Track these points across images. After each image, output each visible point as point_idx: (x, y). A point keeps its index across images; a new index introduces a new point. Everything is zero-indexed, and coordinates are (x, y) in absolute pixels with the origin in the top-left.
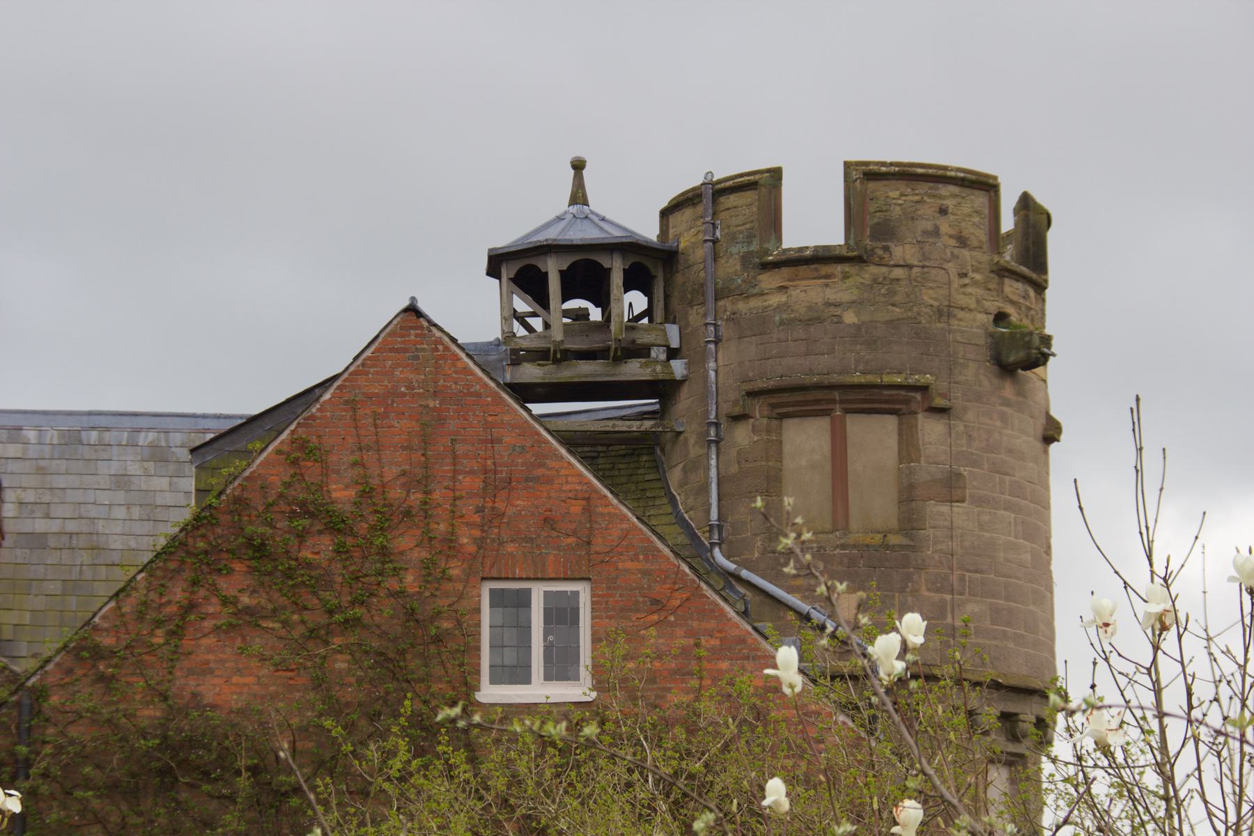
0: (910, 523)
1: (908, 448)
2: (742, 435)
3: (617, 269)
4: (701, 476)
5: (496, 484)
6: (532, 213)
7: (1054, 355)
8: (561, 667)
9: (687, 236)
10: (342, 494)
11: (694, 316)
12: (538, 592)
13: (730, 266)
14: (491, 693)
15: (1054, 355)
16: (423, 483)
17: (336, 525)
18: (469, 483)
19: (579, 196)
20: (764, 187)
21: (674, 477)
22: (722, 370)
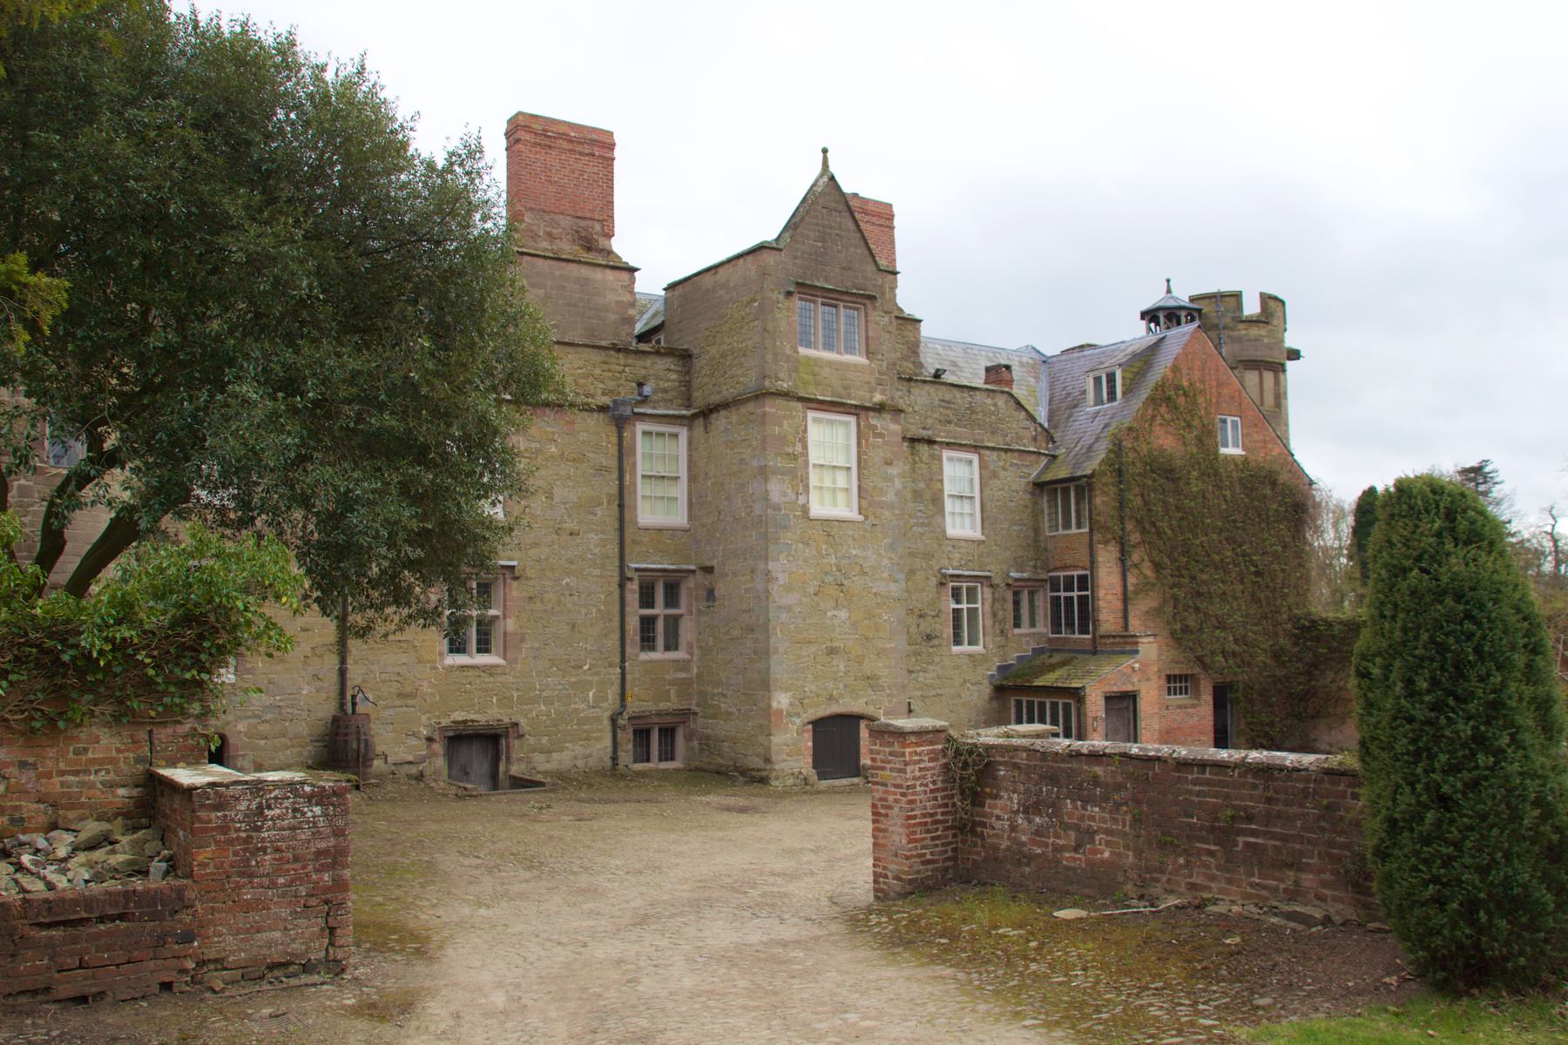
3: (1183, 314)
5: (1219, 385)
6: (1154, 297)
7: (1294, 355)
9: (1206, 307)
10: (1185, 384)
12: (1229, 419)
13: (1227, 320)
14: (1223, 451)
15: (1294, 355)
16: (1203, 382)
18: (1214, 383)
19: (1169, 291)
20: (1237, 296)
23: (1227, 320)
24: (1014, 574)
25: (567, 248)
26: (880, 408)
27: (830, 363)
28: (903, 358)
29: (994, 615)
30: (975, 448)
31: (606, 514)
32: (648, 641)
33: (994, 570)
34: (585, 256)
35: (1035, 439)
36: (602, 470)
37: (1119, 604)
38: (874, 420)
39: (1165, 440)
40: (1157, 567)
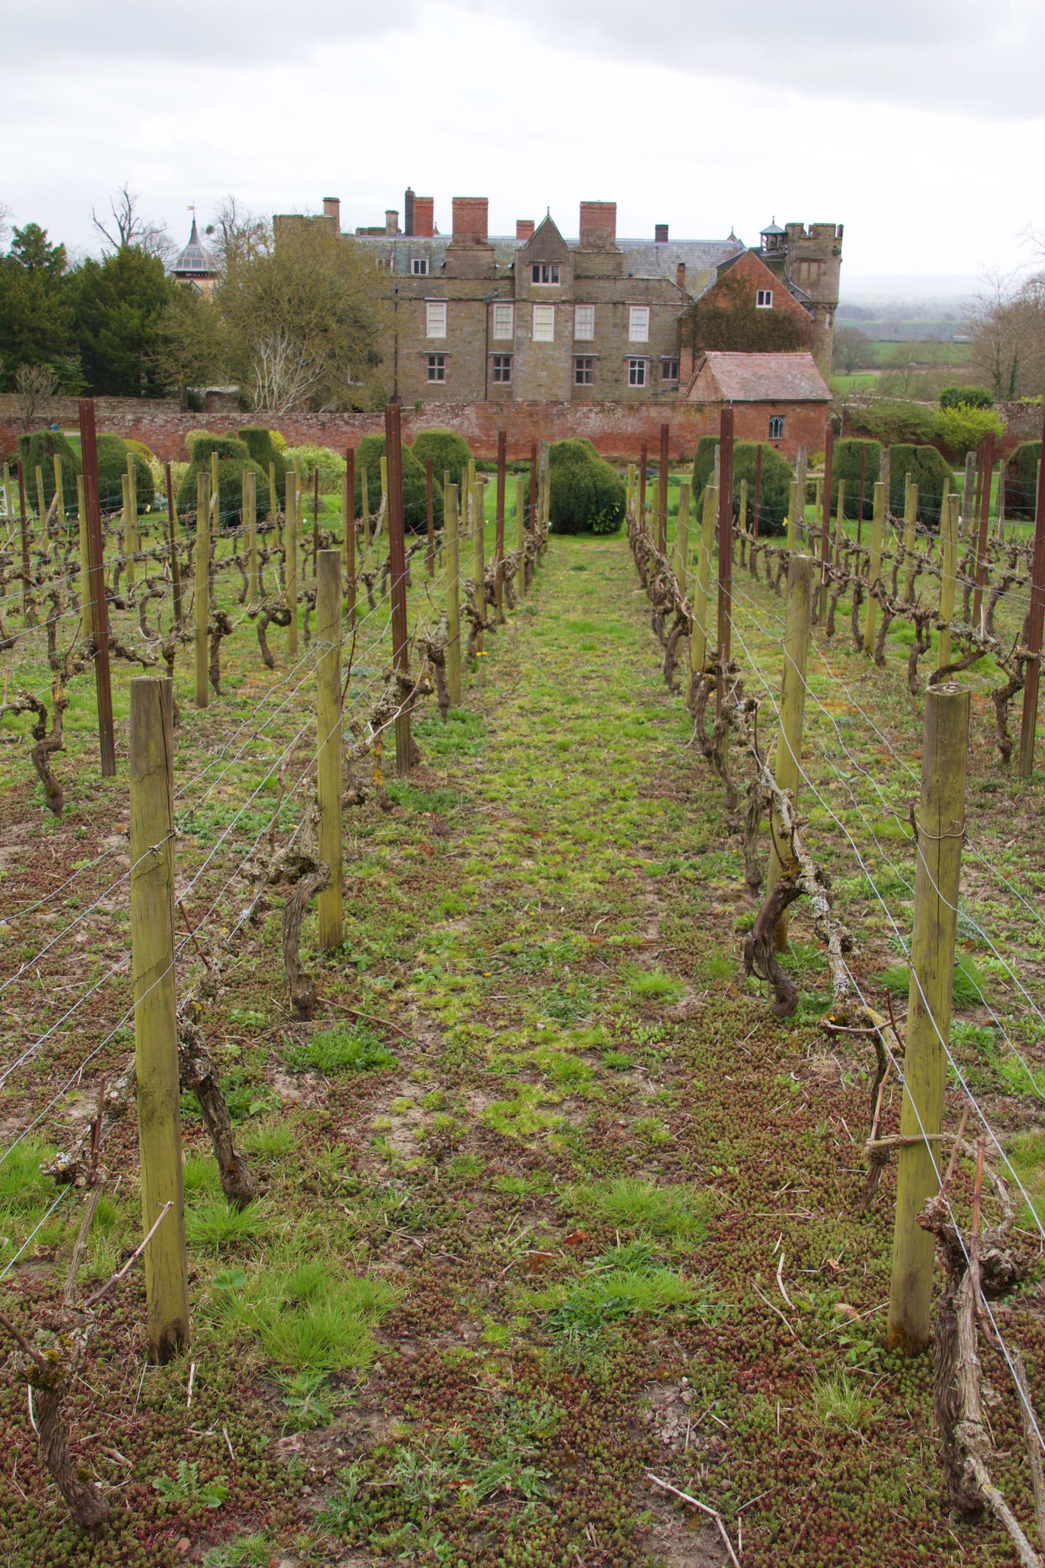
0: (819, 279)
4: (789, 270)
8: (768, 302)
9: (790, 231)
14: (758, 306)
22: (794, 253)
25: (470, 244)
26: (564, 302)
31: (481, 336)
32: (497, 378)
33: (654, 355)
34: (476, 247)
36: (480, 321)
38: (562, 307)
39: (723, 304)
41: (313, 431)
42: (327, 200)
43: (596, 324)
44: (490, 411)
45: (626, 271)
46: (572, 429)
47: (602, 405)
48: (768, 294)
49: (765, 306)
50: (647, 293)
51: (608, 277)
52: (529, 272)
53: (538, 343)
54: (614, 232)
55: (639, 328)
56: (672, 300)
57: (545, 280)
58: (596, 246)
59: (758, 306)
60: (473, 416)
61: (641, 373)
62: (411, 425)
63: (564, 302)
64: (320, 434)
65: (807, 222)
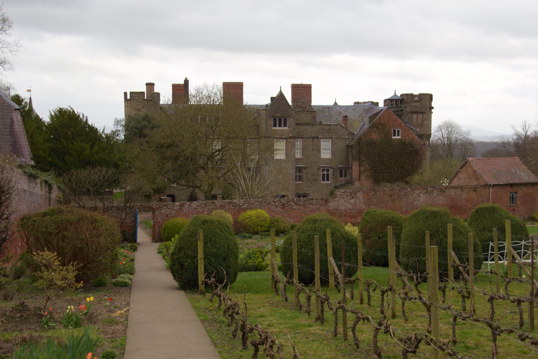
0: (423, 122)
1: (423, 116)
2: (410, 115)
8: (398, 135)
9: (405, 97)
10: (382, 122)
11: (405, 104)
14: (393, 137)
17: (382, 125)
21: (403, 117)
22: (408, 109)
23: (409, 101)
24: (339, 166)
26: (290, 138)
27: (279, 130)
28: (312, 120)
29: (333, 175)
30: (330, 138)
35: (348, 135)
37: (358, 174)
38: (290, 140)
39: (375, 137)
40: (370, 166)
41: (278, 209)
42: (147, 84)
43: (303, 149)
44: (370, 194)
45: (318, 121)
46: (411, 203)
47: (427, 189)
48: (398, 131)
49: (397, 137)
50: (329, 132)
51: (308, 124)
52: (271, 122)
53: (277, 160)
54: (310, 100)
55: (326, 150)
56: (343, 135)
57: (280, 126)
58: (301, 107)
59: (393, 137)
60: (361, 198)
61: (328, 175)
62: (329, 204)
63: (290, 138)
64: (281, 211)
65: (416, 93)
